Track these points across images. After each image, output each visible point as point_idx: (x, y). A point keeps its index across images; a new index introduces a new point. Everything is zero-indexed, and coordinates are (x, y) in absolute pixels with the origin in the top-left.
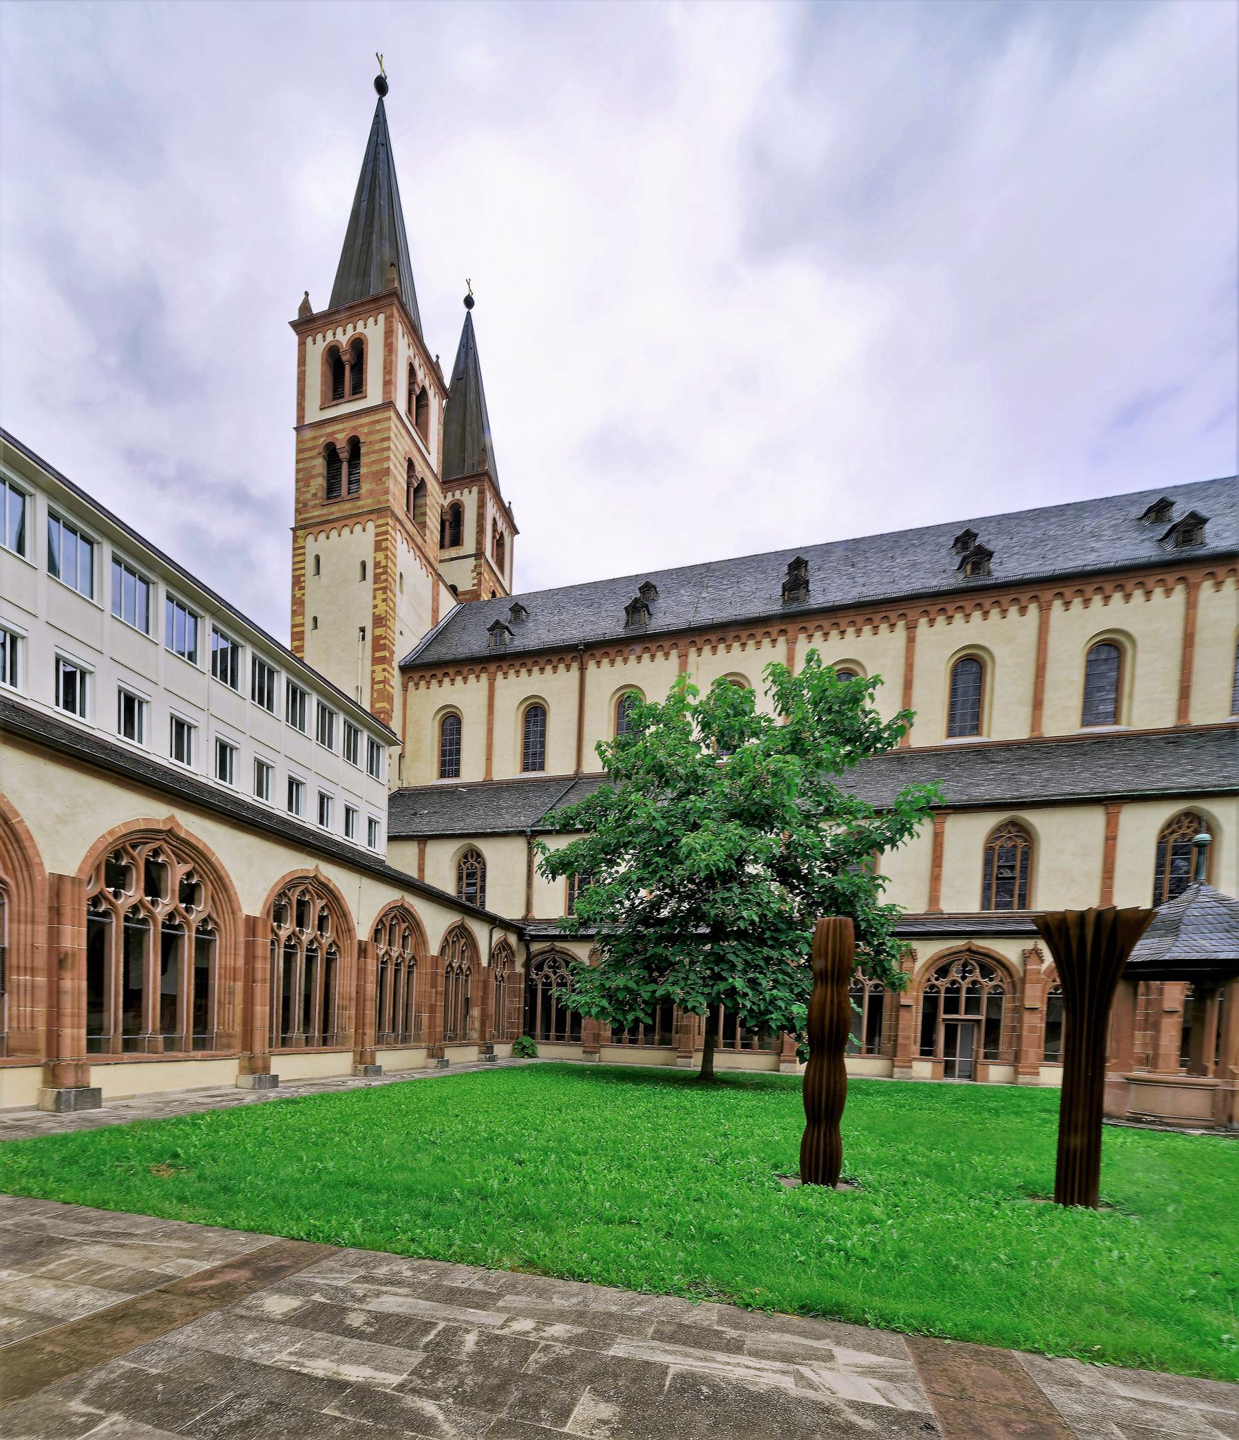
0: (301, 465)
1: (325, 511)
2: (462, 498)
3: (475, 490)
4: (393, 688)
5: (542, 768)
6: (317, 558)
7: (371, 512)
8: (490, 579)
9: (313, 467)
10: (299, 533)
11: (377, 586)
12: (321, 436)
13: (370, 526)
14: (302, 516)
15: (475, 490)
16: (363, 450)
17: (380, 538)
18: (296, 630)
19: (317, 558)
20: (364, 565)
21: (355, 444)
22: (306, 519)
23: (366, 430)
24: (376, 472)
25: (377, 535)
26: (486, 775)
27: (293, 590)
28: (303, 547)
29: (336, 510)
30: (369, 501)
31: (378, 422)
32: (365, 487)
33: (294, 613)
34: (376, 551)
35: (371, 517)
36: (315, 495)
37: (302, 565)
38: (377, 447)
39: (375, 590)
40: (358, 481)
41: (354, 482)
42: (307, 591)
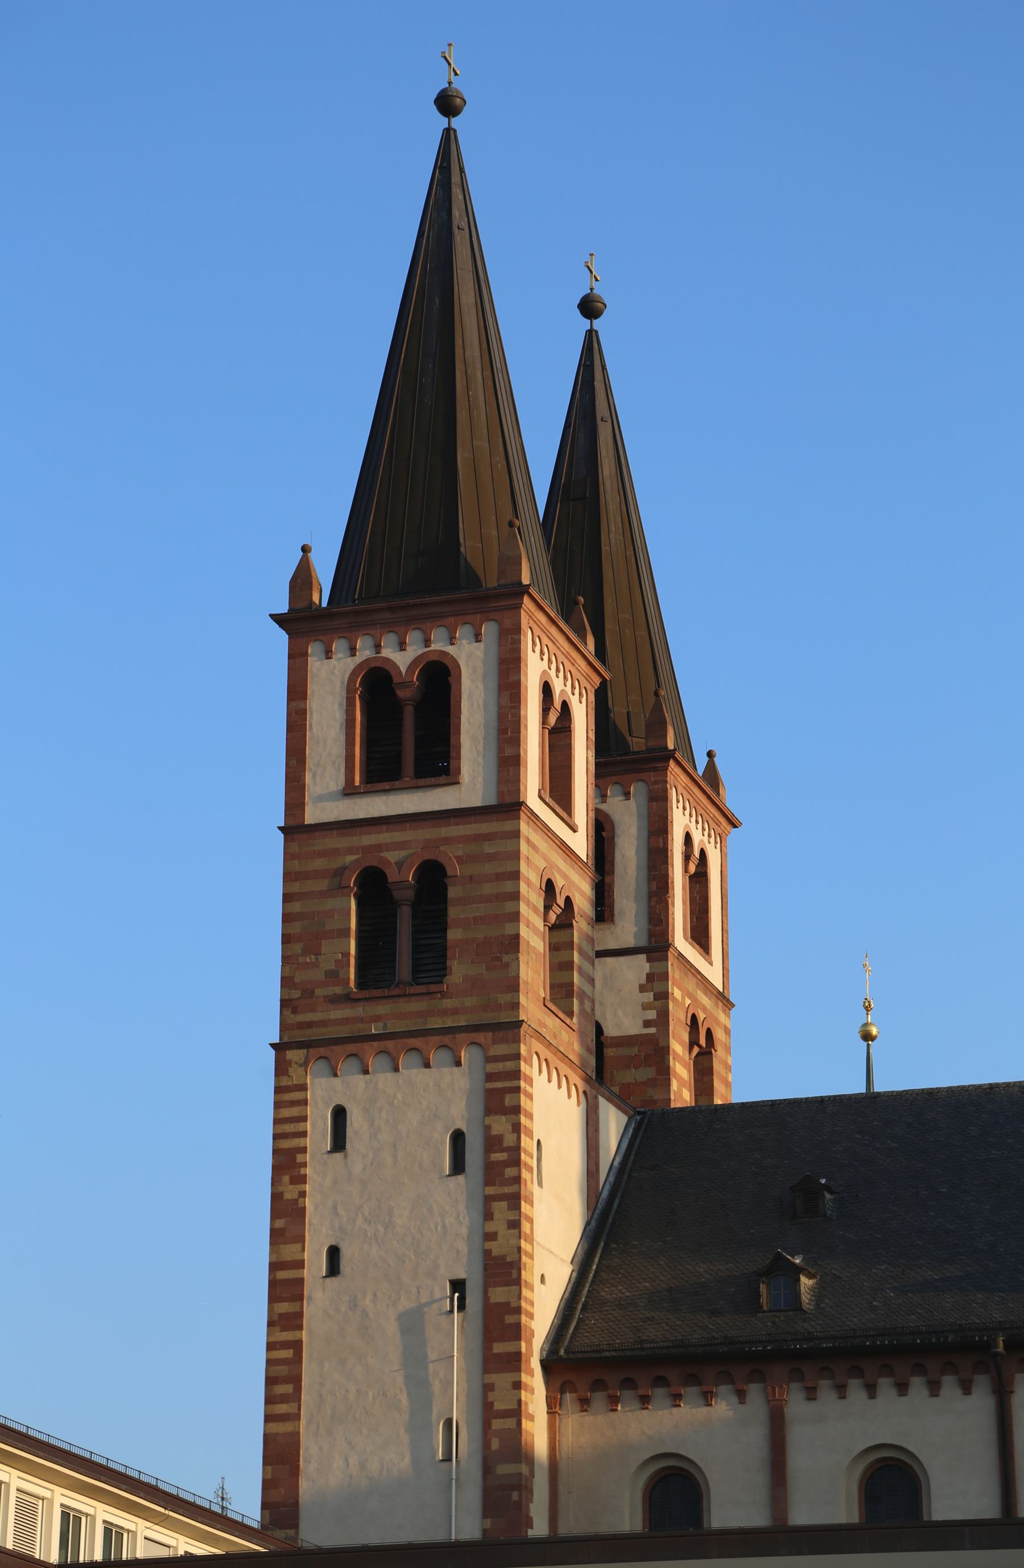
1: (358, 1011)
6: (340, 1114)
12: (350, 851)
17: (499, 1085)
19: (340, 1114)
23: (460, 850)
31: (489, 837)
32: (458, 970)
38: (488, 889)
39: (488, 1200)
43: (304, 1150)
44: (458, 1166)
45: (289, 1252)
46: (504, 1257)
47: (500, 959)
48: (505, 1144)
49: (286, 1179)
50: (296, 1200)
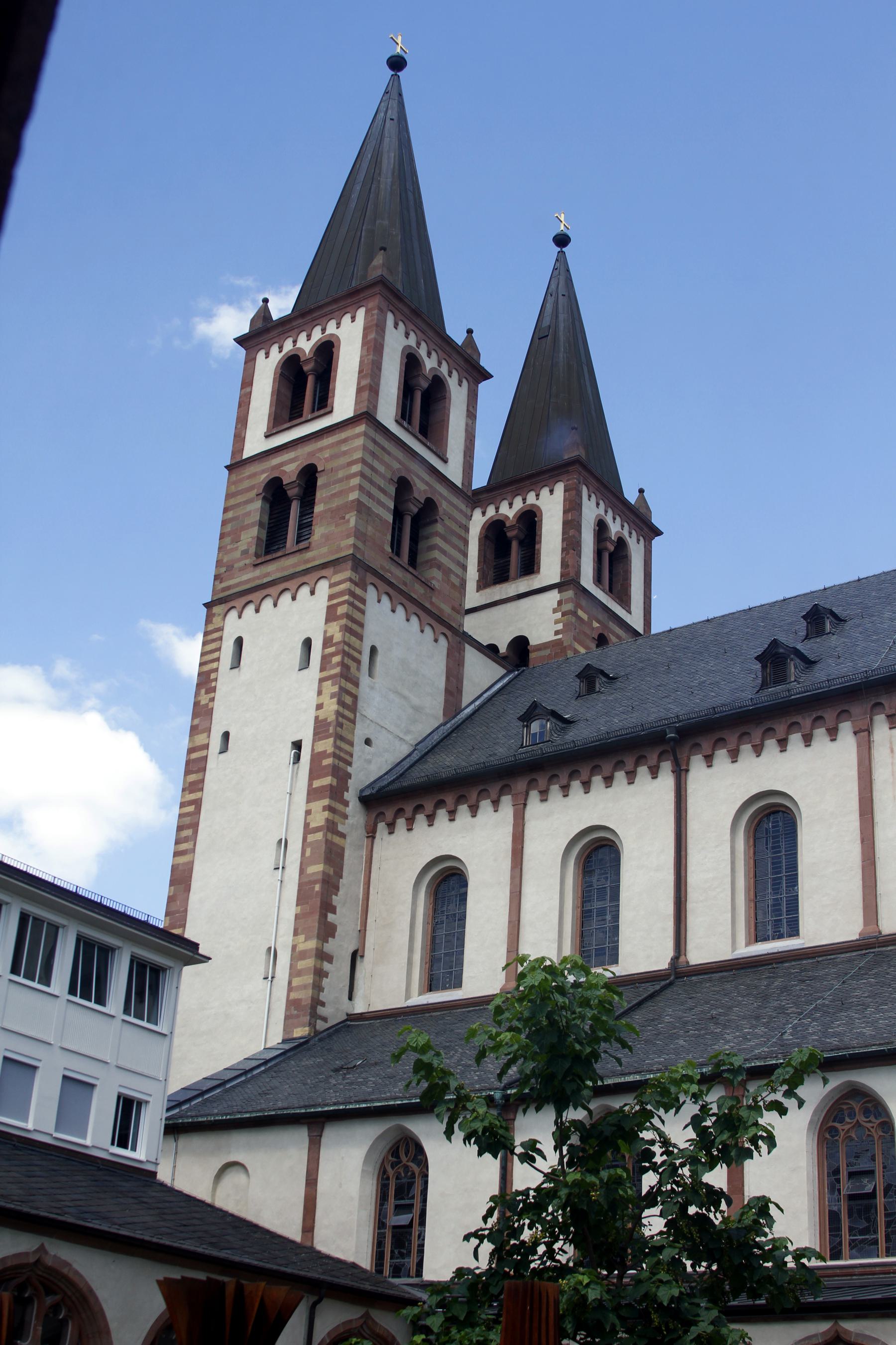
0: (230, 514)
1: (258, 572)
2: (538, 503)
3: (560, 488)
4: (343, 836)
5: (794, 932)
6: (239, 642)
7: (324, 566)
8: (592, 618)
9: (248, 514)
10: (216, 610)
11: (325, 674)
12: (263, 472)
13: (323, 587)
14: (224, 585)
15: (560, 488)
16: (320, 482)
17: (335, 601)
18: (194, 756)
19: (239, 642)
20: (308, 643)
21: (309, 475)
22: (228, 588)
23: (327, 454)
24: (338, 508)
25: (331, 597)
26: (866, 922)
27: (197, 694)
28: (221, 629)
29: (273, 570)
30: (324, 550)
31: (345, 441)
32: (319, 531)
33: (194, 730)
34: (328, 620)
35: (324, 573)
36: (245, 553)
37: (215, 655)
38: (341, 474)
39: (321, 681)
40: (310, 525)
41: (305, 527)
42: (218, 695)
43: (216, 670)
44: (305, 663)
45: (200, 739)
46: (326, 719)
47: (344, 518)
48: (334, 641)
49: (203, 691)
50: (207, 704)
